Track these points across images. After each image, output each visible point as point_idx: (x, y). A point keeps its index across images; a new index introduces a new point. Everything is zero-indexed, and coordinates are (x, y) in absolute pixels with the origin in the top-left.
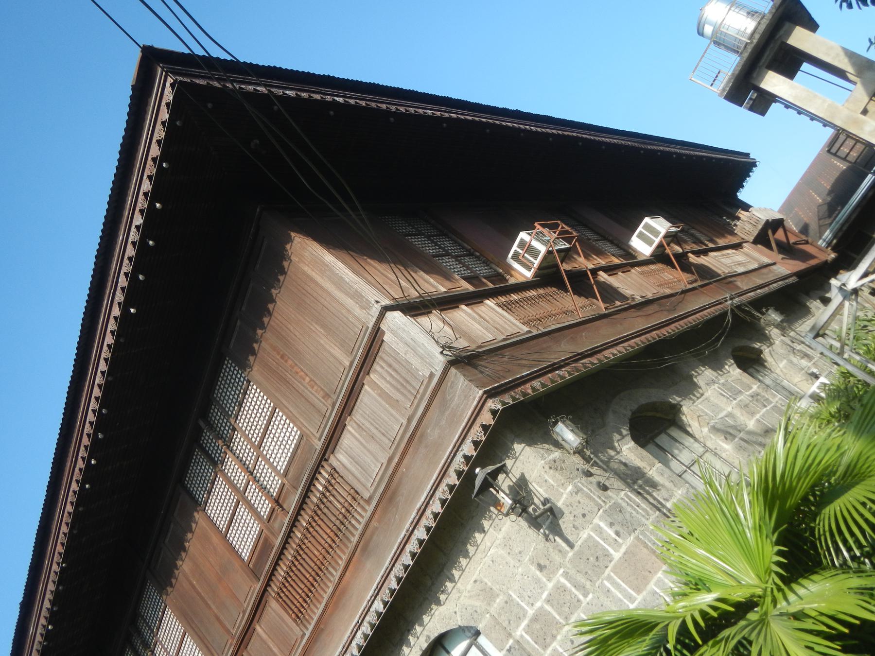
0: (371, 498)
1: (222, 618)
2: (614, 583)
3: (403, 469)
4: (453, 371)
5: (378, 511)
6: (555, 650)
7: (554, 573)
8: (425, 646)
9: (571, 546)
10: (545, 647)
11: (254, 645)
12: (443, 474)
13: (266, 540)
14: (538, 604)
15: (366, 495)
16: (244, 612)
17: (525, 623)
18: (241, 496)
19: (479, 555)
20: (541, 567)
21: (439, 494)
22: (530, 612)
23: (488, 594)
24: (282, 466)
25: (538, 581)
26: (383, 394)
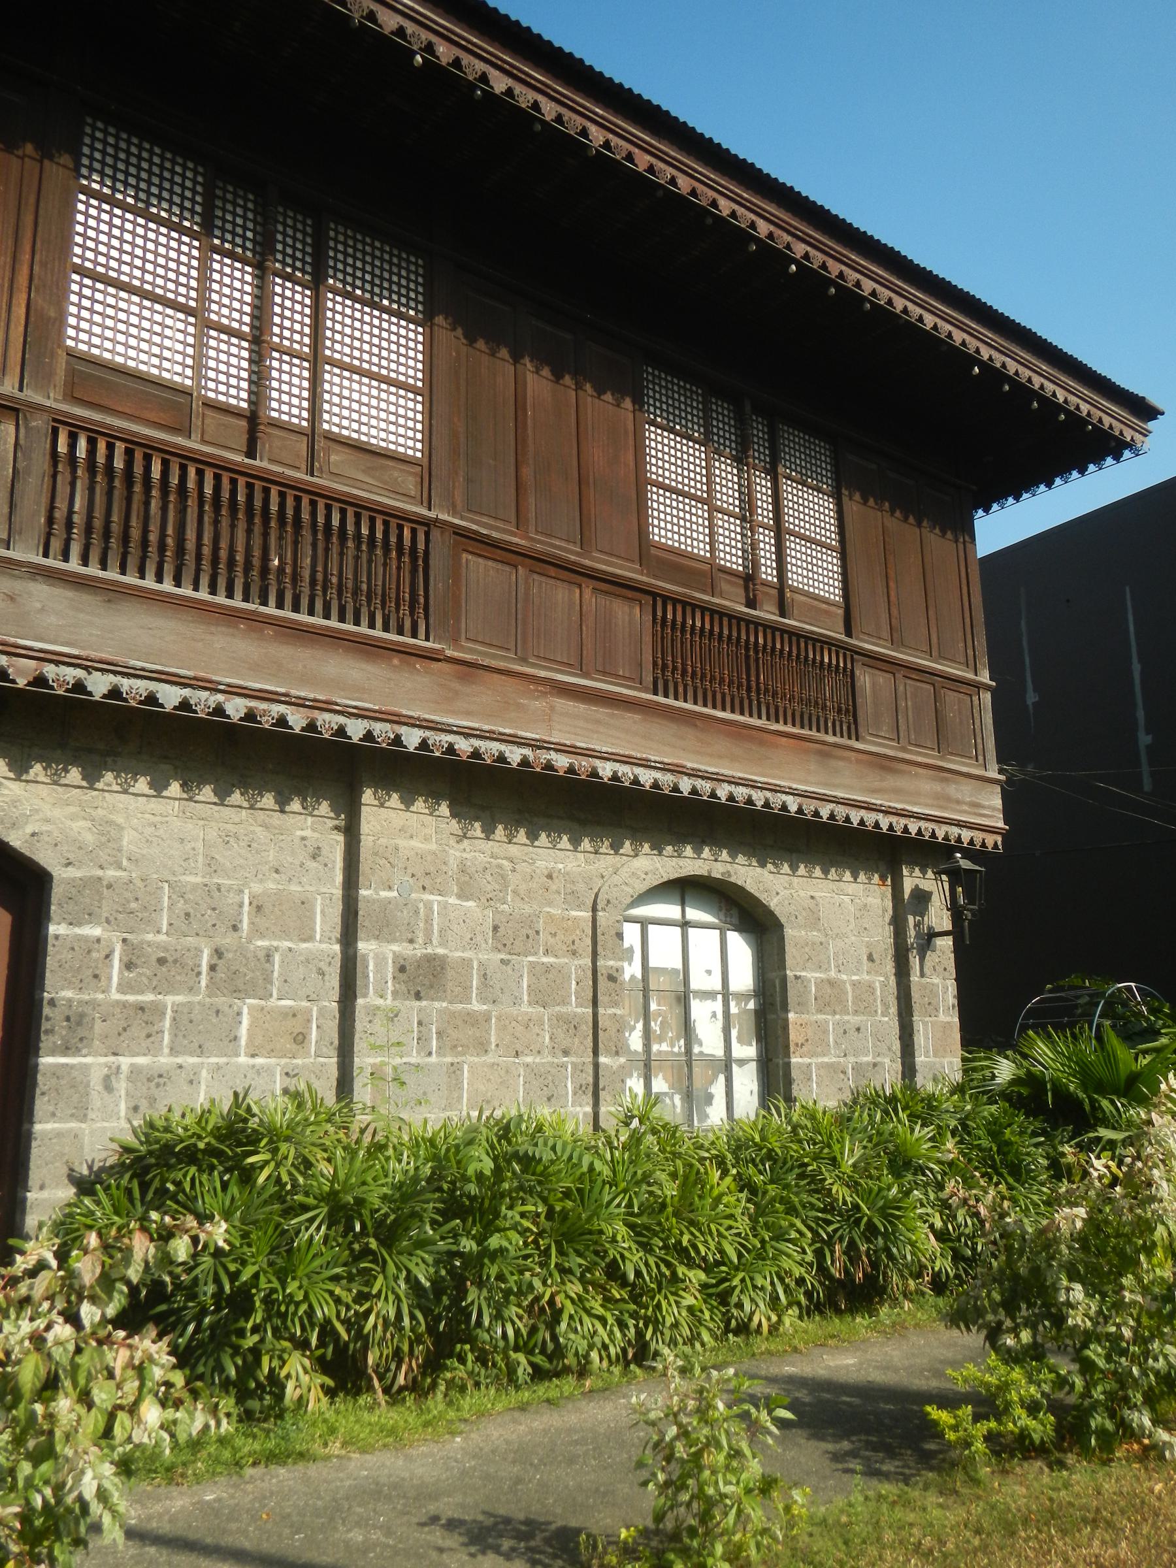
2: (926, 1030)
3: (914, 770)
4: (999, 789)
5: (865, 757)
6: (827, 1022)
7: (877, 973)
8: (716, 875)
9: (922, 975)
10: (820, 1011)
14: (844, 977)
15: (861, 730)
17: (822, 975)
19: (832, 885)
20: (870, 958)
22: (833, 974)
23: (814, 920)
25: (859, 961)
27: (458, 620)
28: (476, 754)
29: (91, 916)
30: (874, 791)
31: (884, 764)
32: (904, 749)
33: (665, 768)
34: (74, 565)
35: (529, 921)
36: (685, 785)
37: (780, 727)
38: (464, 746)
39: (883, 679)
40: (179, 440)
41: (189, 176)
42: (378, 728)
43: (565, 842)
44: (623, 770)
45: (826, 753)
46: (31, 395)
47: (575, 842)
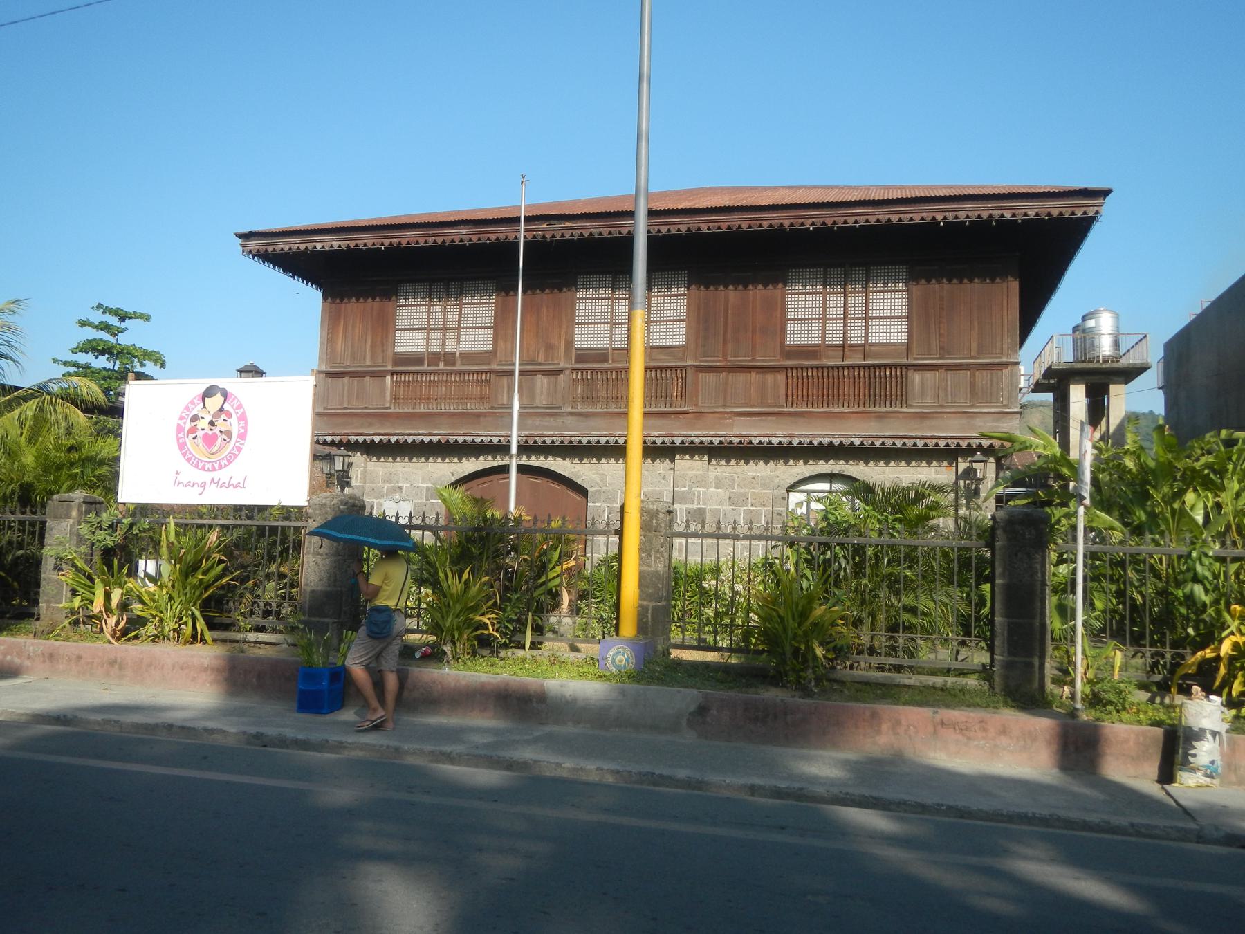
0: (911, 406)
1: (730, 346)
11: (741, 377)
12: (963, 438)
13: (815, 352)
16: (753, 360)
18: (824, 319)
21: (950, 441)
24: (872, 340)
26: (972, 385)
27: (697, 397)
28: (702, 442)
29: (598, 501)
30: (912, 430)
31: (922, 416)
32: (942, 406)
33: (785, 436)
34: (579, 410)
35: (745, 495)
36: (795, 442)
37: (856, 409)
38: (697, 440)
39: (929, 375)
40: (605, 365)
41: (608, 279)
42: (666, 439)
43: (762, 463)
44: (763, 439)
45: (881, 417)
46: (567, 366)
47: (766, 463)
